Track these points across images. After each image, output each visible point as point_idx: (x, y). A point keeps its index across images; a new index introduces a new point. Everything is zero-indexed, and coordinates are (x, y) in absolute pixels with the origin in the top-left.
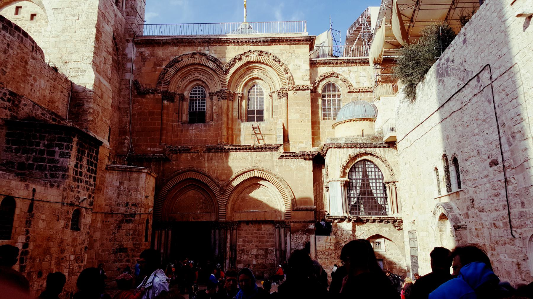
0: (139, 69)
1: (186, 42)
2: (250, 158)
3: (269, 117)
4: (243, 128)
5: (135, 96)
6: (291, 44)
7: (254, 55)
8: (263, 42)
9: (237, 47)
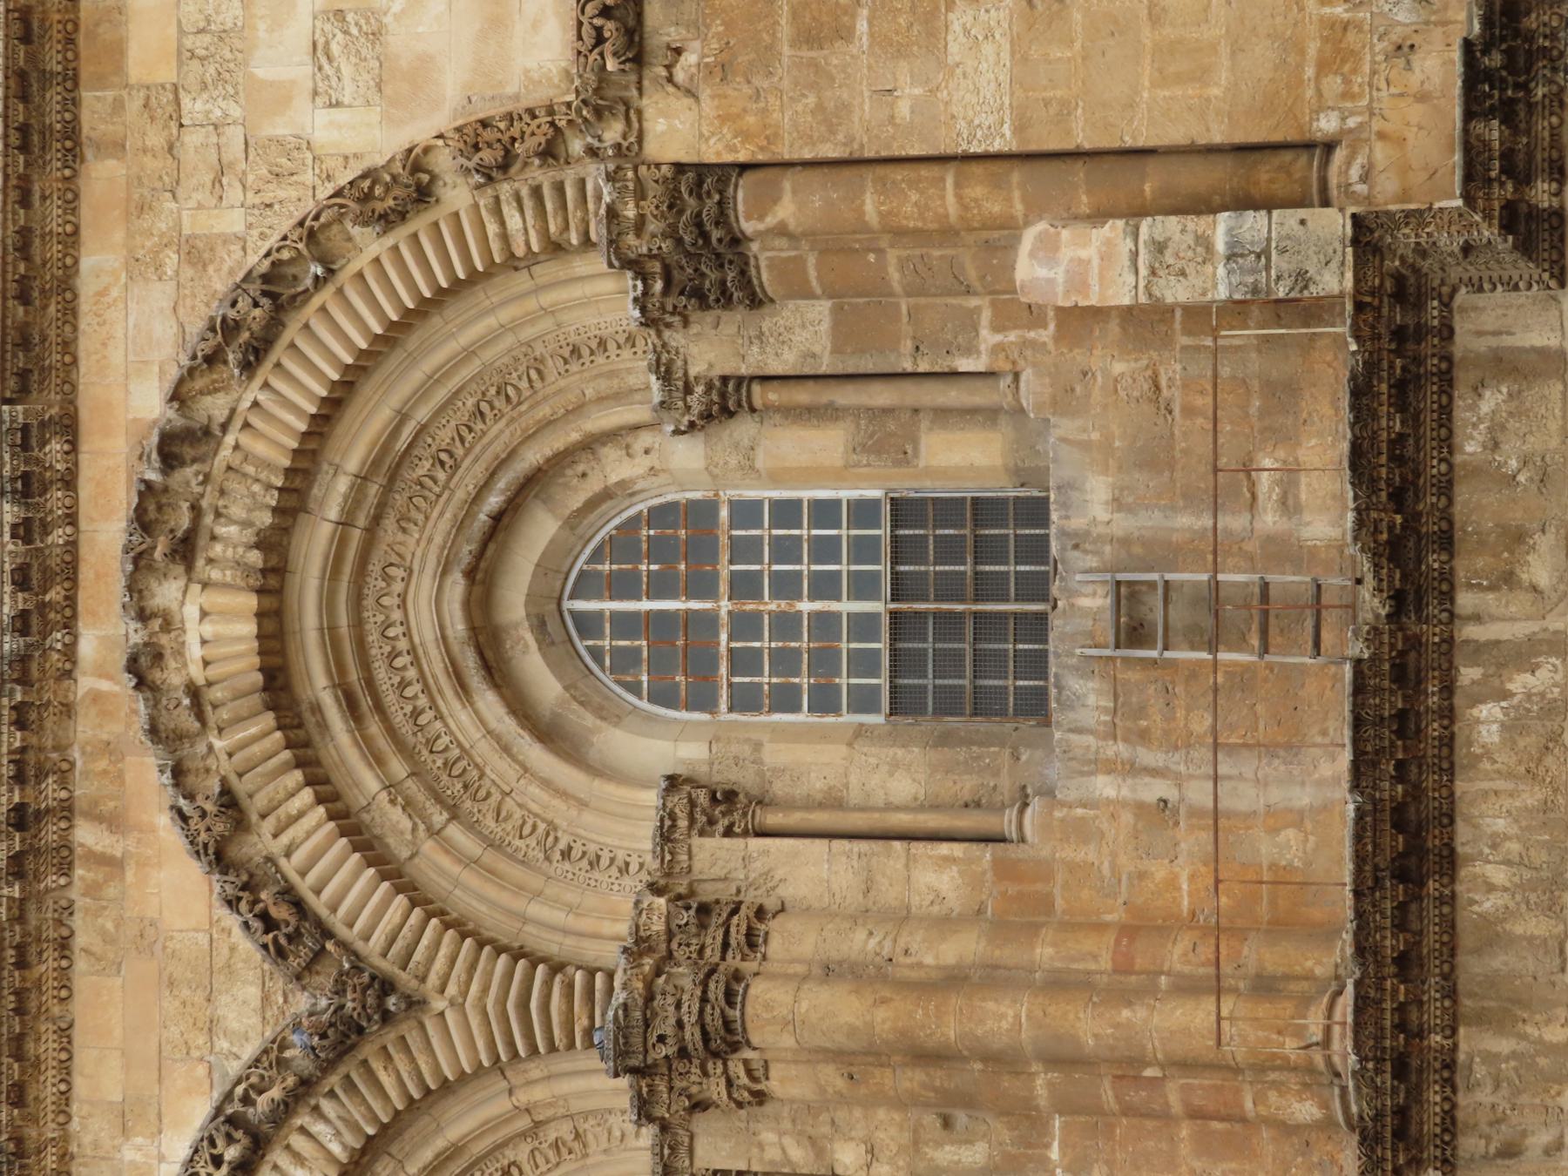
3: (988, 416)
4: (1132, 769)
6: (72, 132)
7: (191, 611)
9: (86, 835)
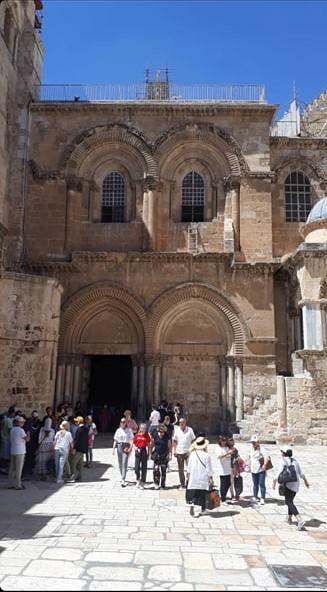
0: (35, 145)
1: (102, 109)
2: (186, 270)
5: (30, 182)
8: (207, 111)
